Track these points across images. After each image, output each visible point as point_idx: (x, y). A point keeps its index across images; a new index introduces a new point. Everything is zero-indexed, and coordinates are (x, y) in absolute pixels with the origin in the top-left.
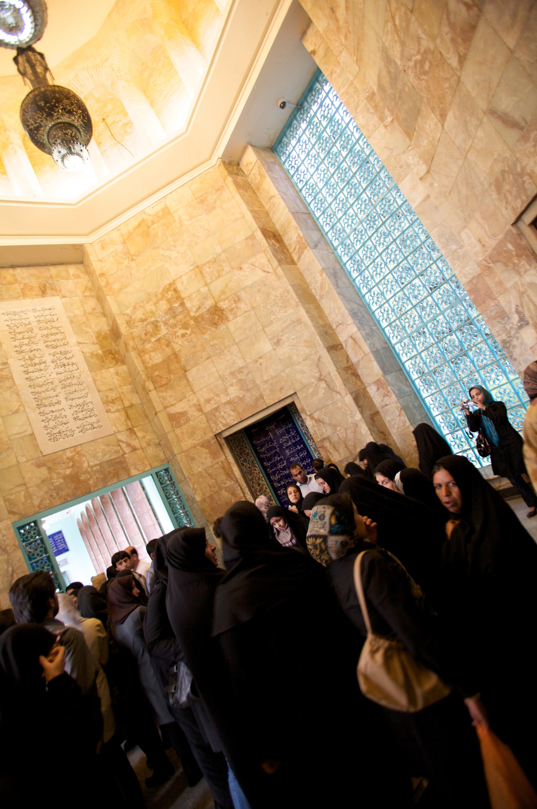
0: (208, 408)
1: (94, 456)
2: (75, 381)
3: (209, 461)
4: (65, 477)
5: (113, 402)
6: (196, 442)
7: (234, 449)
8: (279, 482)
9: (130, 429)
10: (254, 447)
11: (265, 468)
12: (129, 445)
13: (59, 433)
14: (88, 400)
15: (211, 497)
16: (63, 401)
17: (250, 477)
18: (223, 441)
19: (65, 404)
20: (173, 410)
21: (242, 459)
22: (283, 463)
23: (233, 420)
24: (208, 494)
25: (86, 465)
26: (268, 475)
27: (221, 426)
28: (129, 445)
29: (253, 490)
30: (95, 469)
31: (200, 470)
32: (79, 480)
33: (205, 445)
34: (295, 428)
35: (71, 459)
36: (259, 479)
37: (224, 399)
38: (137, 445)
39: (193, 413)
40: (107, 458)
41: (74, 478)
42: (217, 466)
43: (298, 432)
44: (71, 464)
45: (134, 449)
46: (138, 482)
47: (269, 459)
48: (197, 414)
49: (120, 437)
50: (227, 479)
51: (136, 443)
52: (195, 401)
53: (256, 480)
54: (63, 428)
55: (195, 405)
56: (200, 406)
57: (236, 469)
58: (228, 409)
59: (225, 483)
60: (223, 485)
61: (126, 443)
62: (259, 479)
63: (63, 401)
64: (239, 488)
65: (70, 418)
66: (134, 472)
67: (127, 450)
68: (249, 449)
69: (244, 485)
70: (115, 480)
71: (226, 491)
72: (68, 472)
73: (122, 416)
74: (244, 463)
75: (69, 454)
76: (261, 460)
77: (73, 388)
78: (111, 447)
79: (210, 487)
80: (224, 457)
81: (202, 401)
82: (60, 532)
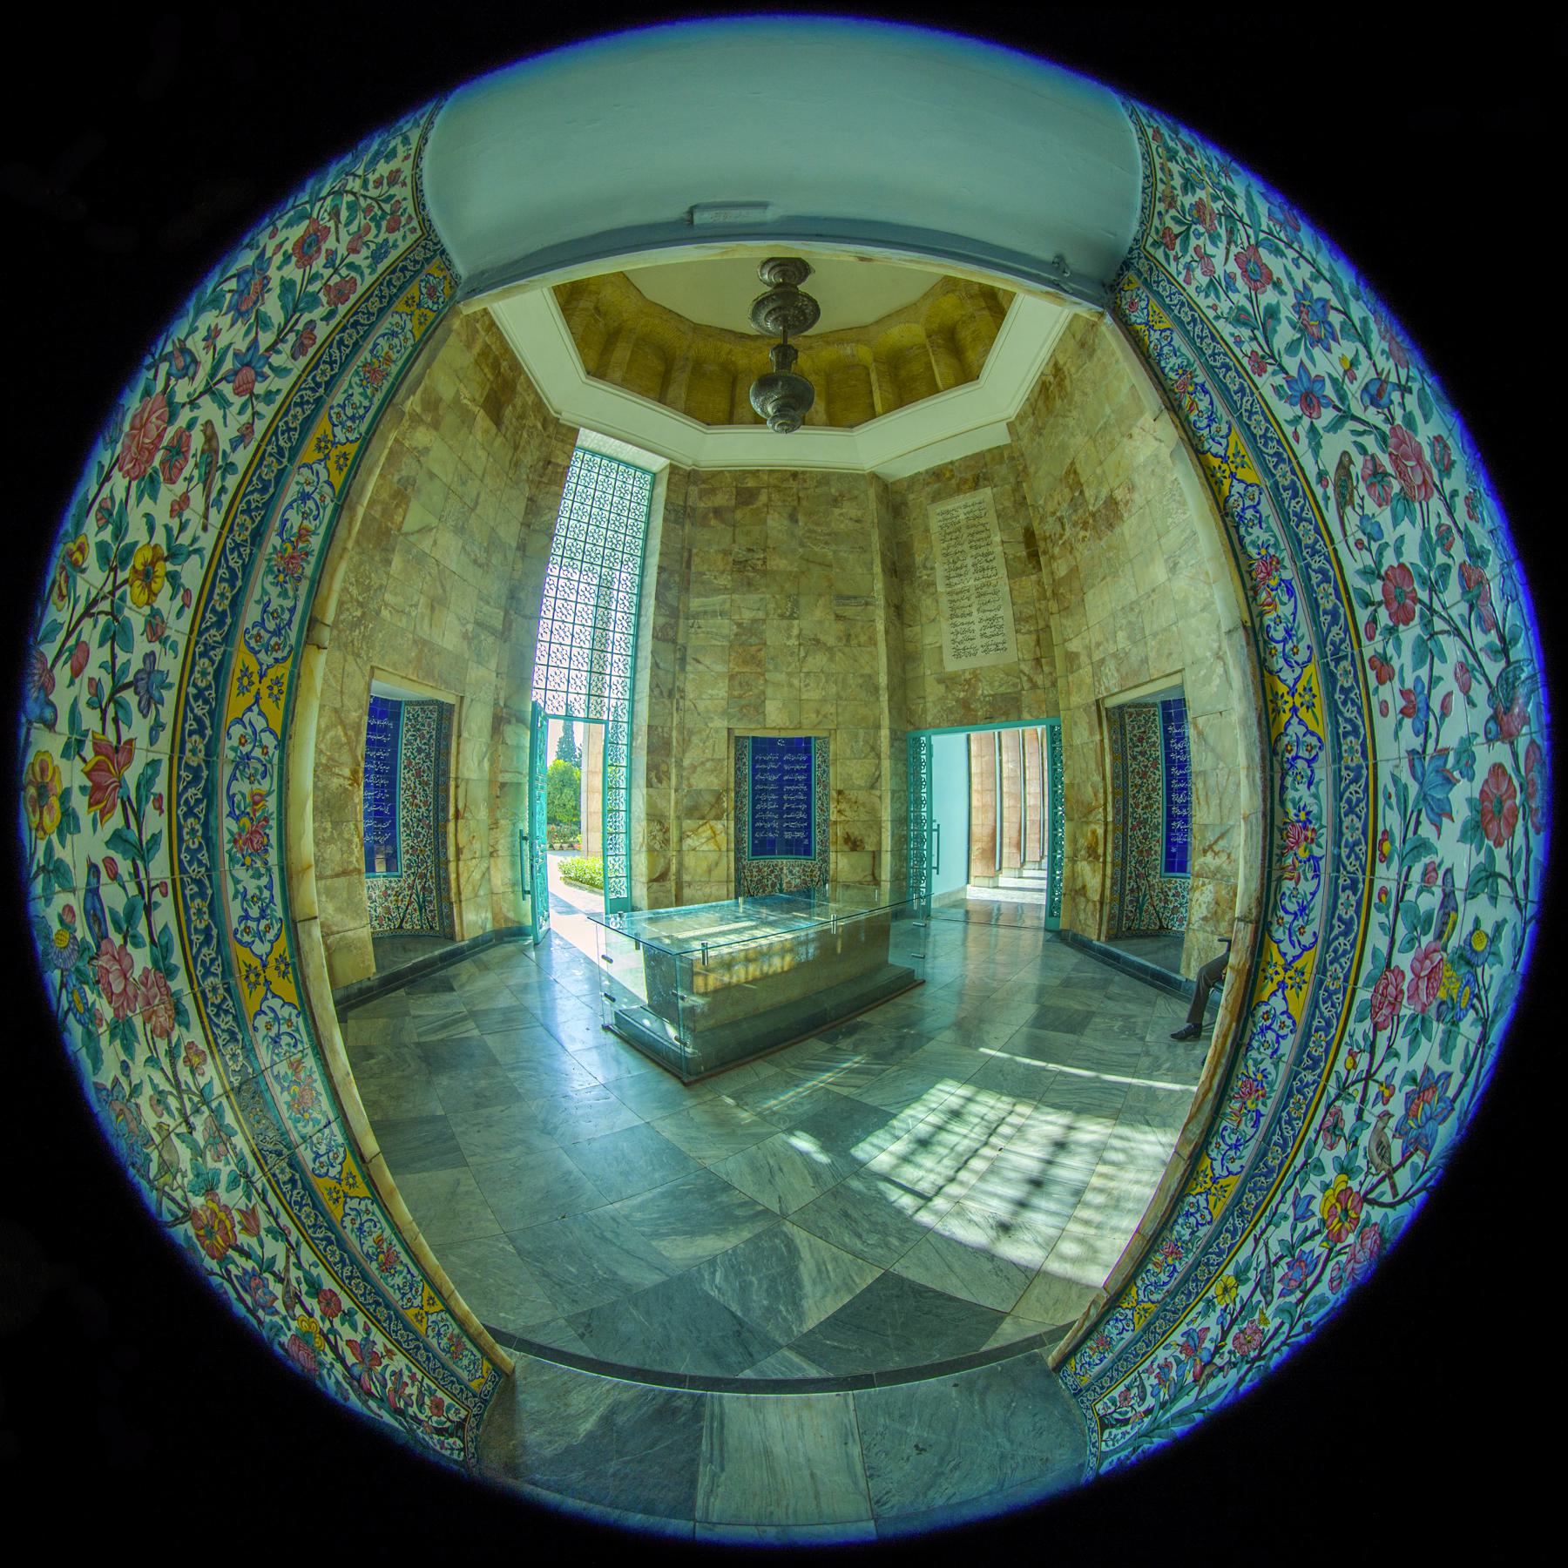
2: (991, 589)
5: (1027, 620)
7: (1128, 728)
14: (1000, 613)
16: (975, 613)
17: (1138, 781)
19: (976, 616)
26: (1169, 790)
28: (1030, 679)
29: (1131, 801)
35: (968, 682)
36: (1154, 789)
37: (1112, 649)
38: (1040, 683)
40: (1002, 690)
41: (965, 704)
45: (1034, 686)
46: (963, 736)
49: (1022, 666)
51: (1039, 679)
62: (1154, 789)
63: (975, 613)
65: (977, 633)
66: (1026, 715)
67: (1027, 685)
72: (962, 695)
73: (1032, 639)
75: (967, 676)
77: (988, 598)
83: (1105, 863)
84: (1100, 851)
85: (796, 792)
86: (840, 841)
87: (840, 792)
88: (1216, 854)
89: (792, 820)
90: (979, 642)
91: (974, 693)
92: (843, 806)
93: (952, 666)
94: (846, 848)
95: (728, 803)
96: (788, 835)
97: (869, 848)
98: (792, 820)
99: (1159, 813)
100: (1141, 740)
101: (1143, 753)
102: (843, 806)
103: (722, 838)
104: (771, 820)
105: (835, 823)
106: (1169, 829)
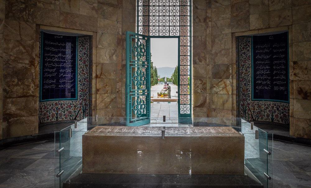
17: (242, 63)
53: (246, 67)
74: (243, 55)
85: (280, 64)
89: (279, 80)
96: (276, 88)
98: (279, 80)
100: (244, 48)
101: (244, 53)
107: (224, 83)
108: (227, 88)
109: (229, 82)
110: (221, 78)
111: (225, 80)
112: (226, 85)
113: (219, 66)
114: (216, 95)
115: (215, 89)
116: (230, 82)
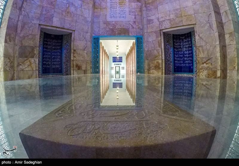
0: (161, 20)
1: (120, 26)
3: (155, 38)
4: (110, 29)
6: (153, 31)
7: (166, 38)
8: (177, 58)
9: (135, 22)
10: (174, 42)
11: (174, 51)
12: (132, 26)
13: (113, 16)
15: (151, 51)
18: (162, 33)
20: (149, 18)
21: (167, 44)
22: (182, 52)
23: (167, 27)
24: (150, 50)
25: (117, 27)
26: (174, 54)
27: (163, 27)
28: (132, 26)
29: (166, 55)
30: (119, 29)
31: (151, 40)
32: (113, 31)
33: (155, 32)
34: (191, 41)
36: (170, 53)
39: (156, 20)
40: (124, 27)
41: (112, 30)
42: (157, 41)
43: (191, 43)
44: (113, 26)
45: (133, 28)
47: (177, 49)
48: (157, 21)
50: (158, 47)
51: (135, 26)
52: (158, 17)
54: (115, 15)
55: (157, 18)
56: (159, 18)
57: (163, 44)
58: (168, 22)
59: (157, 48)
60: (156, 48)
61: (132, 25)
62: (170, 53)
64: (161, 51)
68: (171, 42)
69: (163, 51)
70: (124, 35)
71: (156, 51)
72: (111, 27)
73: (134, 17)
75: (114, 23)
76: (174, 48)
78: (126, 25)
79: (152, 47)
80: (160, 39)
81: (160, 17)
82: (122, 57)
83: (162, 69)
84: (161, 66)
86: (75, 66)
87: (75, 50)
88: (207, 64)
90: (118, 15)
91: (115, 27)
92: (75, 55)
93: (109, 19)
94: (76, 69)
95: (36, 52)
96: (54, 67)
97: (84, 68)
99: (172, 59)
102: (75, 55)
103: (33, 65)
104: (48, 61)
105: (73, 60)
106: (174, 63)
107: (30, 61)
108: (32, 65)
109: (34, 61)
110: (26, 57)
111: (30, 59)
112: (31, 63)
113: (25, 47)
114: (22, 72)
115: (21, 67)
116: (34, 60)
